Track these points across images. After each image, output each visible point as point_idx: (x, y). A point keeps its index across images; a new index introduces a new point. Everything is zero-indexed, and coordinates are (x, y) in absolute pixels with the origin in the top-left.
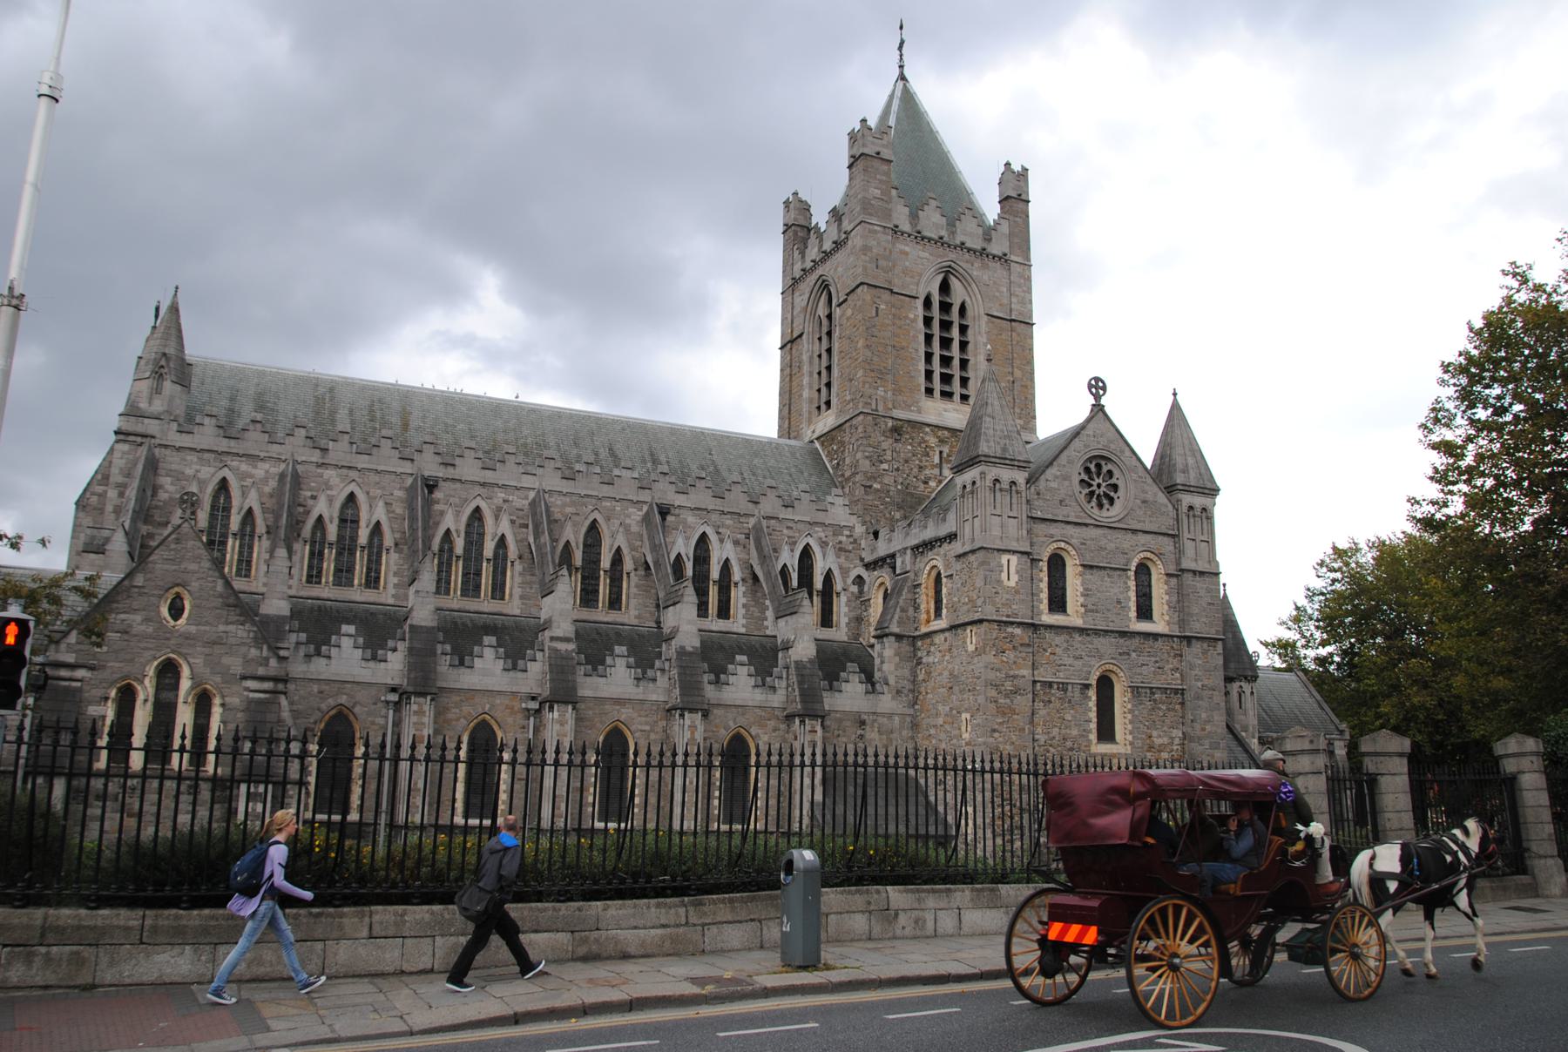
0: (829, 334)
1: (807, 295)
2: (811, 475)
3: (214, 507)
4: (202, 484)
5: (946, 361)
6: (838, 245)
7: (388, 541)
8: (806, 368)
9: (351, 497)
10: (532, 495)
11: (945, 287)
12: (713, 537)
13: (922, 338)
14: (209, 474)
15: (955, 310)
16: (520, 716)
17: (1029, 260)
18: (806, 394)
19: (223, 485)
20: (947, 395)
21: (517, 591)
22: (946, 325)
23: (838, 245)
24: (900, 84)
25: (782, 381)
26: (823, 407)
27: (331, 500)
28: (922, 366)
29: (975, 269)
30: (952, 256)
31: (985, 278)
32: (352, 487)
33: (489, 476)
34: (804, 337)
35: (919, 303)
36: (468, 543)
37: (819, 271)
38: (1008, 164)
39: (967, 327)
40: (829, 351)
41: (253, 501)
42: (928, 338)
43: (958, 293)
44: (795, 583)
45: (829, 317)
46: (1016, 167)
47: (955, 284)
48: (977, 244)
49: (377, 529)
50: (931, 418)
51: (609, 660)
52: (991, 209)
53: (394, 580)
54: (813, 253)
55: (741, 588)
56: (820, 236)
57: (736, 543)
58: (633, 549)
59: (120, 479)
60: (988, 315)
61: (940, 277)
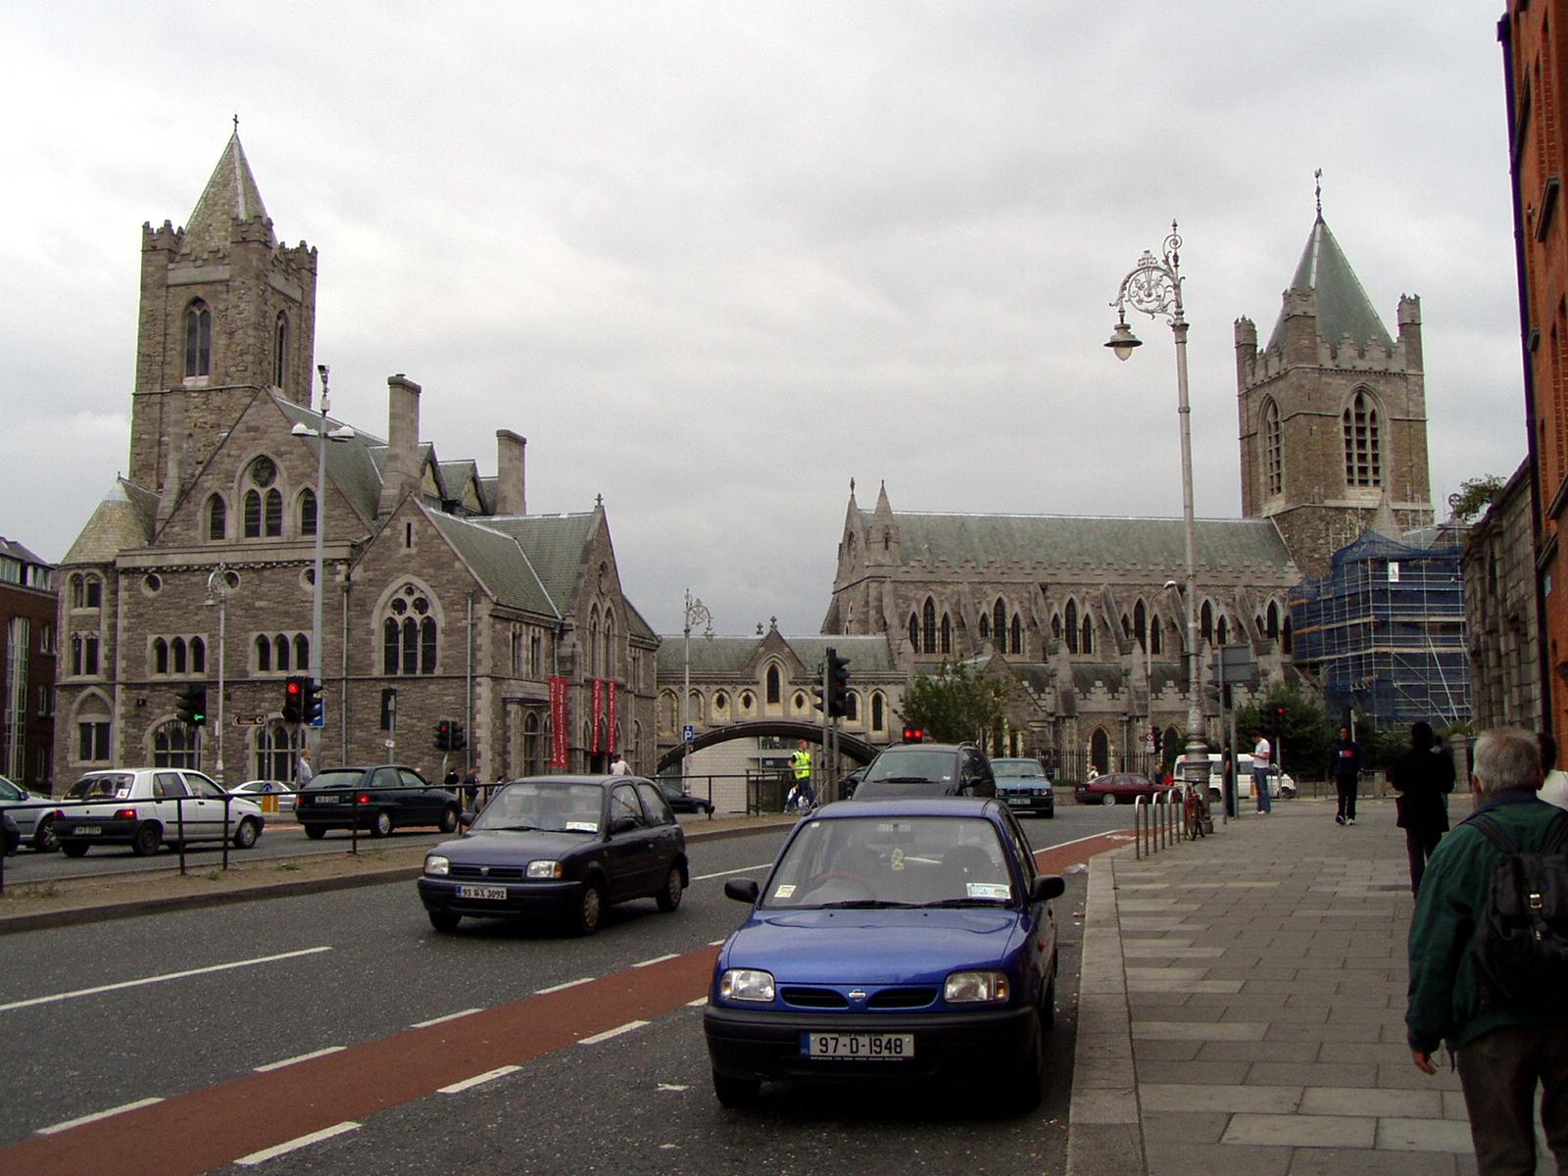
0: (1277, 436)
1: (1258, 404)
2: (1270, 546)
3: (926, 615)
4: (918, 601)
5: (1362, 457)
6: (1280, 377)
7: (1023, 624)
8: (1260, 459)
9: (1000, 600)
10: (1102, 588)
11: (1359, 402)
12: (1213, 603)
13: (1344, 445)
14: (923, 597)
15: (1368, 418)
16: (1118, 725)
17: (1422, 370)
18: (1262, 479)
19: (929, 601)
20: (1364, 482)
21: (1099, 648)
22: (1361, 431)
25: (1243, 464)
26: (1275, 490)
27: (989, 603)
28: (1344, 466)
29: (1382, 387)
30: (1363, 379)
31: (1388, 391)
32: (1000, 594)
33: (1076, 579)
36: (1067, 621)
37: (1267, 390)
38: (1403, 297)
40: (1278, 449)
41: (947, 608)
42: (1348, 443)
44: (1266, 628)
45: (1276, 423)
47: (1367, 398)
49: (1016, 619)
50: (1352, 503)
51: (1164, 689)
52: (1394, 333)
53: (1028, 647)
54: (1260, 375)
55: (1232, 634)
57: (1227, 605)
58: (1165, 615)
59: (875, 604)
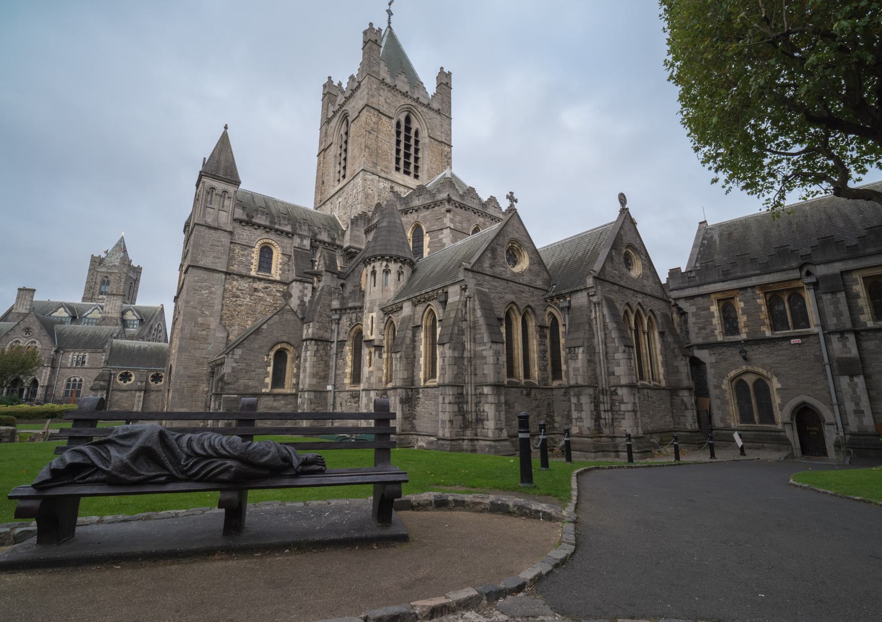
11: (408, 120)
13: (394, 138)
20: (407, 173)
23: (354, 91)
24: (389, 29)
26: (341, 179)
28: (394, 152)
34: (333, 145)
35: (394, 122)
38: (442, 68)
39: (419, 141)
43: (415, 125)
45: (346, 133)
46: (445, 70)
48: (426, 102)
56: (343, 92)
60: (431, 137)
61: (405, 114)
